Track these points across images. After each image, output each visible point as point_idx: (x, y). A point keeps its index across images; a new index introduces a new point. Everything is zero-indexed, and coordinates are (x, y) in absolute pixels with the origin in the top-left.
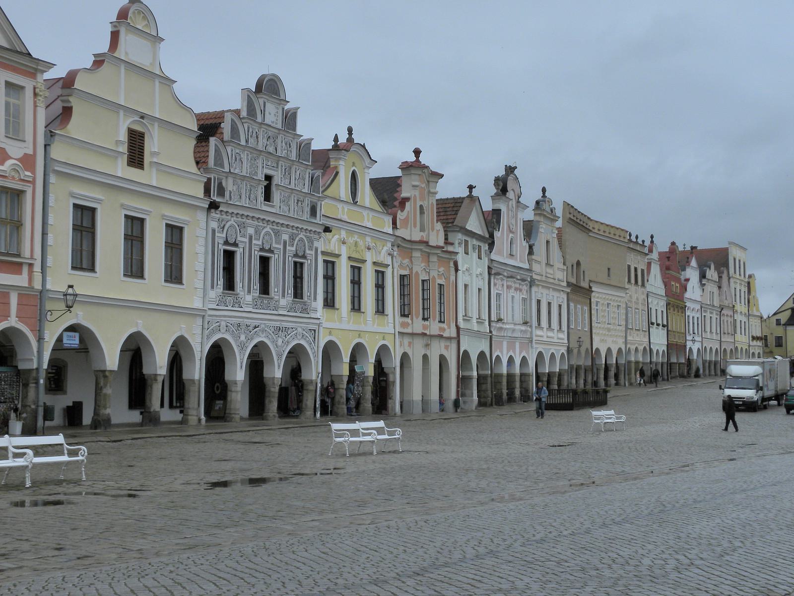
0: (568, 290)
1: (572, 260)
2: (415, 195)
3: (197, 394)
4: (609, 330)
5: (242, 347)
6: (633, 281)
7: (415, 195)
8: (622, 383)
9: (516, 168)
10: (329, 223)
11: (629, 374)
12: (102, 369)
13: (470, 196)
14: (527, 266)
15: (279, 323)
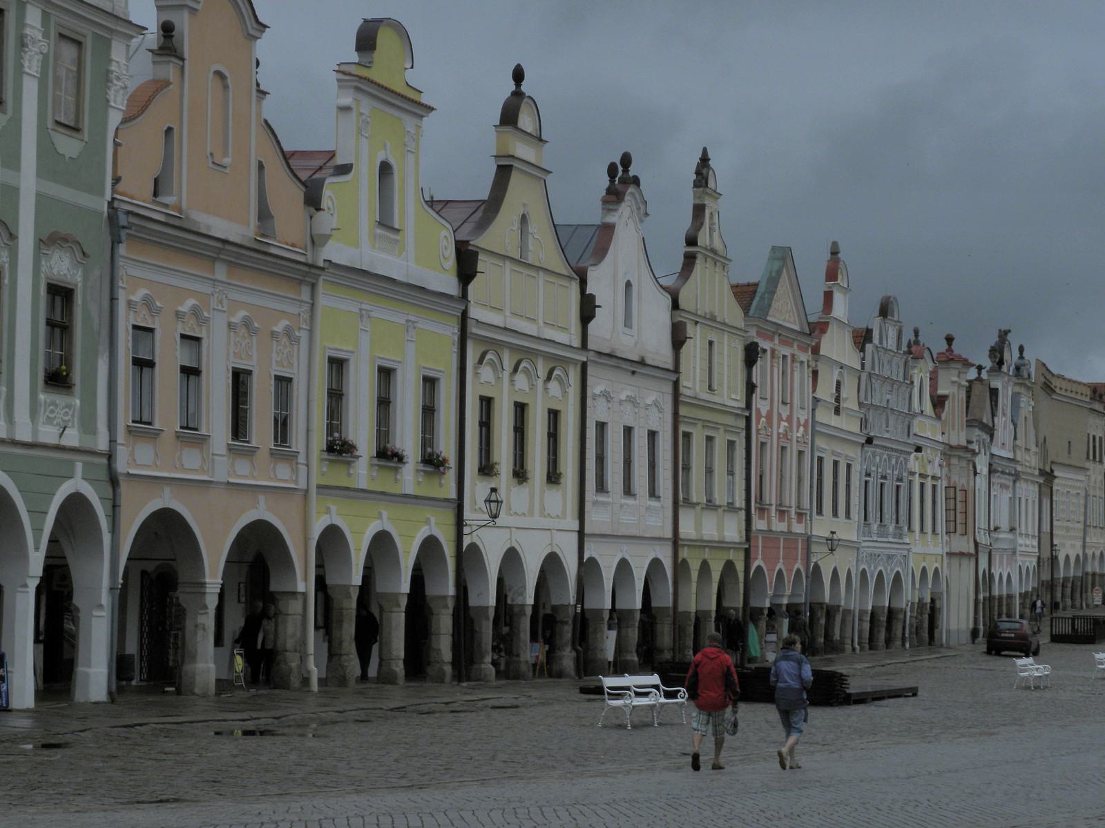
0: (1041, 481)
1: (1041, 440)
2: (953, 393)
3: (851, 624)
4: (1068, 529)
5: (872, 576)
6: (1091, 457)
7: (953, 393)
8: (1078, 605)
9: (1009, 331)
10: (920, 442)
11: (1086, 592)
12: (820, 601)
13: (979, 379)
14: (1010, 455)
15: (889, 551)
